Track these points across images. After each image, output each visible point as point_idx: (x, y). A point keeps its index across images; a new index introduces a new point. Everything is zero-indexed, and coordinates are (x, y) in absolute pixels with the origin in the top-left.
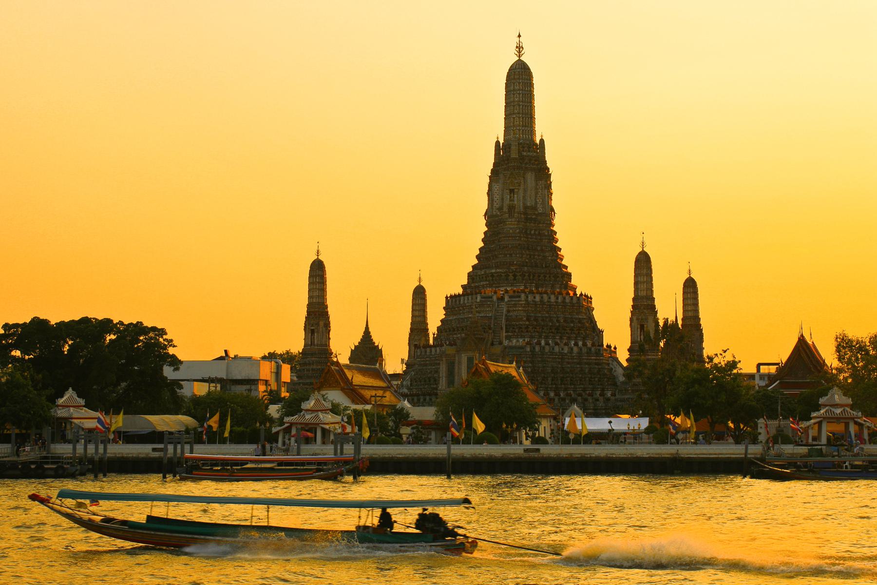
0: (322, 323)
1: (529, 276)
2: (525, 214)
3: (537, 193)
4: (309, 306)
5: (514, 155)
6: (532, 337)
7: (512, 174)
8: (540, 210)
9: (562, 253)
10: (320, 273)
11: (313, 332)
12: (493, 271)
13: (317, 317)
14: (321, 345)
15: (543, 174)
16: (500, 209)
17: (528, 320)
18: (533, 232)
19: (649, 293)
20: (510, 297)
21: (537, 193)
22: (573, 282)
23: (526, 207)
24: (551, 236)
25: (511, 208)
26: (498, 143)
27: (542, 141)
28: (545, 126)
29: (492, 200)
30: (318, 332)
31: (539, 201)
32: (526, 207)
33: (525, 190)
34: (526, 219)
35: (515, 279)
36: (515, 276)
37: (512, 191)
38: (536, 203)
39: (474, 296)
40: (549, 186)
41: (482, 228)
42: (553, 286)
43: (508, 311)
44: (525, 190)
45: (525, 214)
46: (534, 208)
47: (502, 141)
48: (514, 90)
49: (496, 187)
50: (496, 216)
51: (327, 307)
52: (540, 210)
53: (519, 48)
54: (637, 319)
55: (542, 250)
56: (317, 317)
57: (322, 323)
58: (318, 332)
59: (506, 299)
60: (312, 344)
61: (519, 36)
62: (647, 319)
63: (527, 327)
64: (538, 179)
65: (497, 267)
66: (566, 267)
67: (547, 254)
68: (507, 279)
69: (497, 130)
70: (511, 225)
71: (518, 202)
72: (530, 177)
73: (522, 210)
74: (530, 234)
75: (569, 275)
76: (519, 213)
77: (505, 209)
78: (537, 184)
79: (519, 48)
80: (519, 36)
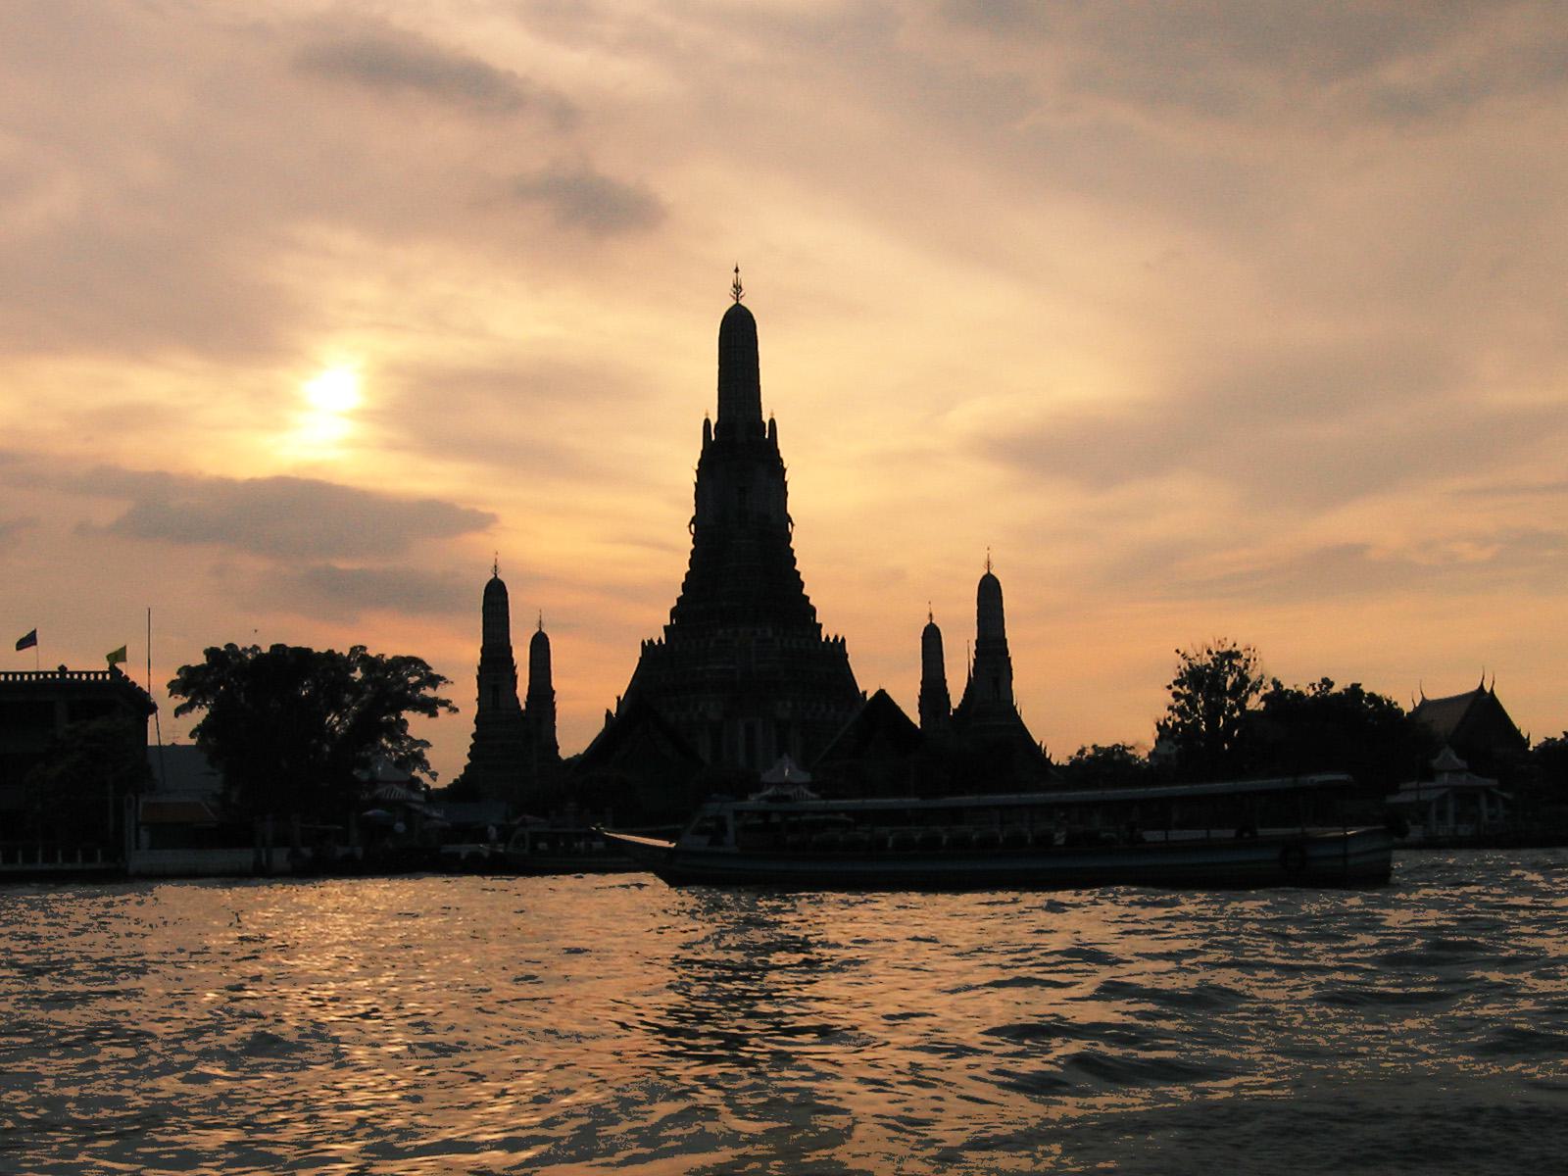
26: (707, 422)
27: (772, 422)
28: (774, 401)
47: (714, 420)
53: (738, 288)
61: (737, 270)
69: (709, 406)
79: (738, 288)
80: (737, 270)
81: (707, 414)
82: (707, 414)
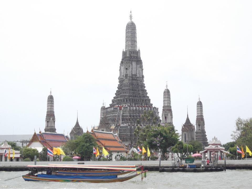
0: (51, 119)
1: (132, 100)
2: (132, 77)
3: (137, 70)
4: (48, 112)
5: (128, 55)
6: (131, 123)
7: (127, 62)
8: (138, 76)
9: (147, 92)
10: (51, 100)
11: (48, 122)
12: (119, 99)
13: (50, 116)
14: (51, 127)
15: (139, 62)
16: (123, 76)
17: (130, 116)
18: (135, 84)
19: (169, 104)
20: (124, 108)
21: (137, 70)
22: (151, 102)
23: (132, 75)
24: (143, 86)
25: (126, 75)
27: (139, 50)
28: (141, 45)
29: (121, 73)
30: (50, 122)
31: (138, 72)
32: (132, 75)
33: (132, 69)
34: (133, 79)
35: (127, 101)
36: (127, 100)
37: (127, 69)
38: (137, 73)
39: (111, 108)
40: (141, 67)
41: (117, 83)
42: (141, 104)
43: (123, 113)
44: (132, 69)
45: (132, 77)
46: (136, 75)
47: (124, 51)
48: (128, 32)
49: (122, 68)
50: (123, 78)
51: (54, 112)
52: (138, 76)
53: (131, 17)
54: (164, 115)
55: (138, 91)
56: (50, 116)
57: (51, 119)
58: (50, 122)
59: (122, 109)
60: (48, 126)
61: (131, 12)
62: (167, 115)
63: (130, 119)
64: (137, 64)
65: (121, 97)
66: (148, 97)
67: (140, 92)
68: (124, 102)
70: (126, 81)
71: (129, 73)
72: (134, 64)
73: (131, 76)
74: (134, 85)
75: (149, 100)
76: (129, 77)
77: (124, 76)
78: (137, 66)
79: (131, 17)
80: (131, 12)
81: (123, 50)
82: (123, 50)
